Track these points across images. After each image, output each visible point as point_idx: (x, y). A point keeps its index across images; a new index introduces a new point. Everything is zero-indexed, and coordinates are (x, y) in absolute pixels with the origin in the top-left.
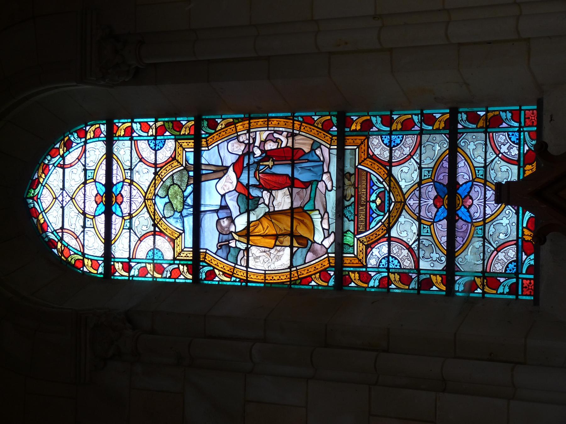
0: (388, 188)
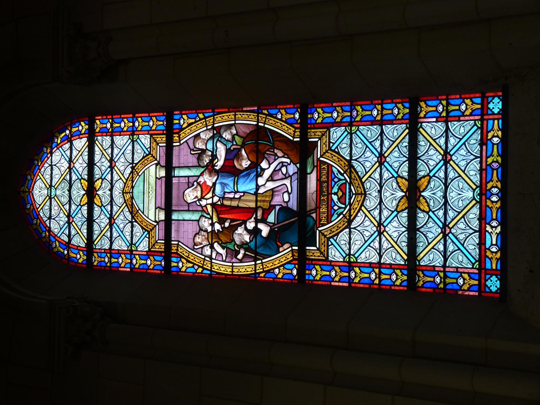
0: (348, 180)
